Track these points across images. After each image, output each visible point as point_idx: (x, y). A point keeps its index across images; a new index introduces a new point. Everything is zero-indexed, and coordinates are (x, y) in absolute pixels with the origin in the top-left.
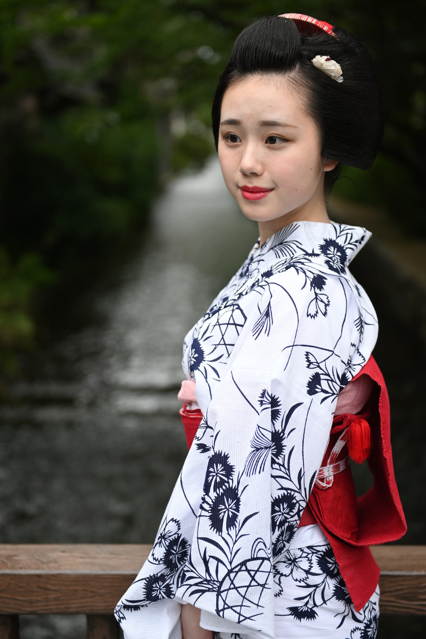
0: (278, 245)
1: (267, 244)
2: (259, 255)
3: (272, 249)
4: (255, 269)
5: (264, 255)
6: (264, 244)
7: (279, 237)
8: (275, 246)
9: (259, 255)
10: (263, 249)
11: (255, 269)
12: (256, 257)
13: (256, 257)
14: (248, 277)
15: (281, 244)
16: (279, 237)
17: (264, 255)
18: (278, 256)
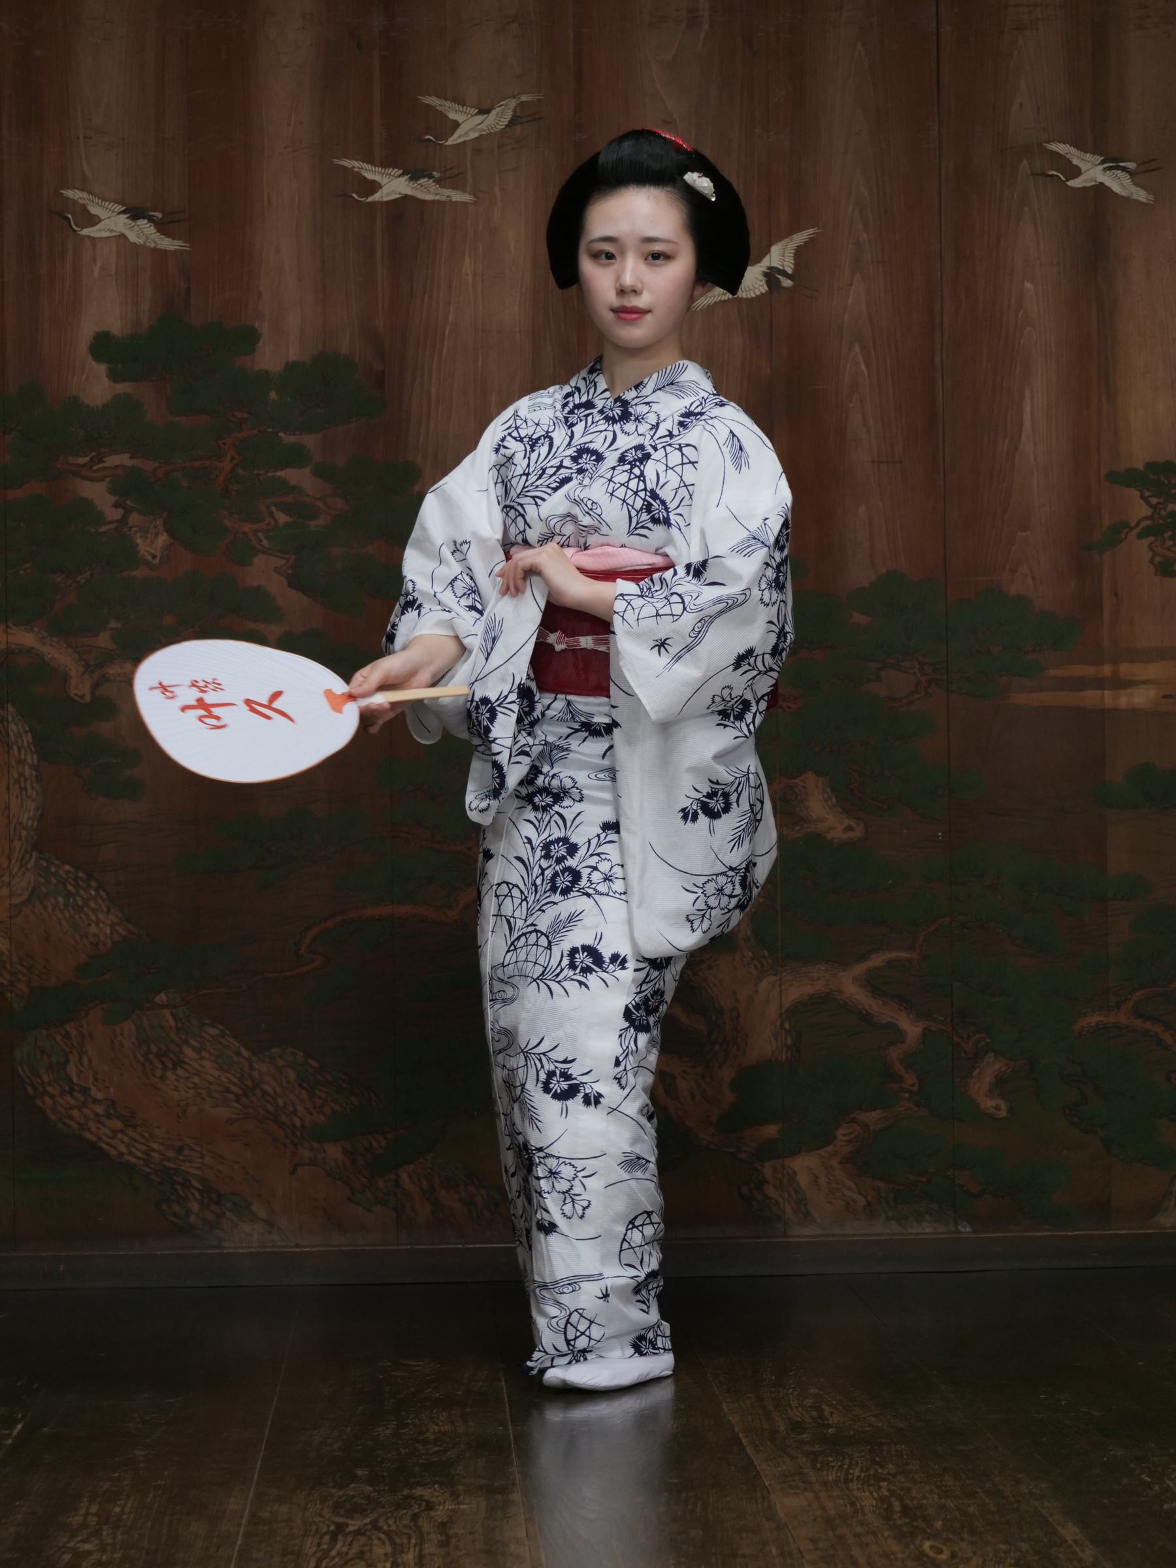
0: (668, 385)
1: (646, 384)
2: (637, 397)
3: (660, 389)
4: (647, 413)
5: (647, 396)
6: (641, 383)
7: (666, 377)
8: (664, 387)
9: (637, 397)
10: (641, 391)
11: (647, 413)
12: (633, 399)
13: (633, 399)
14: (640, 422)
15: (672, 384)
16: (666, 377)
17: (647, 396)
18: (679, 397)
